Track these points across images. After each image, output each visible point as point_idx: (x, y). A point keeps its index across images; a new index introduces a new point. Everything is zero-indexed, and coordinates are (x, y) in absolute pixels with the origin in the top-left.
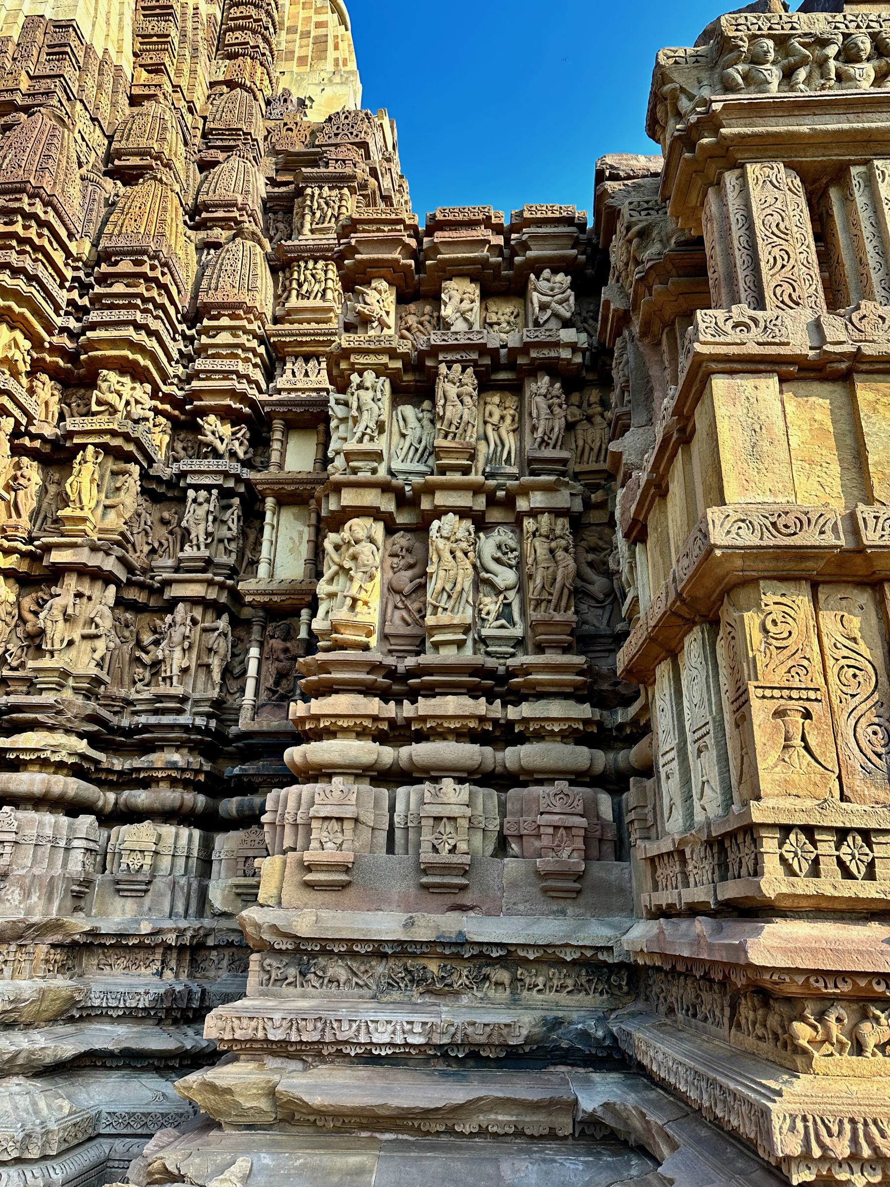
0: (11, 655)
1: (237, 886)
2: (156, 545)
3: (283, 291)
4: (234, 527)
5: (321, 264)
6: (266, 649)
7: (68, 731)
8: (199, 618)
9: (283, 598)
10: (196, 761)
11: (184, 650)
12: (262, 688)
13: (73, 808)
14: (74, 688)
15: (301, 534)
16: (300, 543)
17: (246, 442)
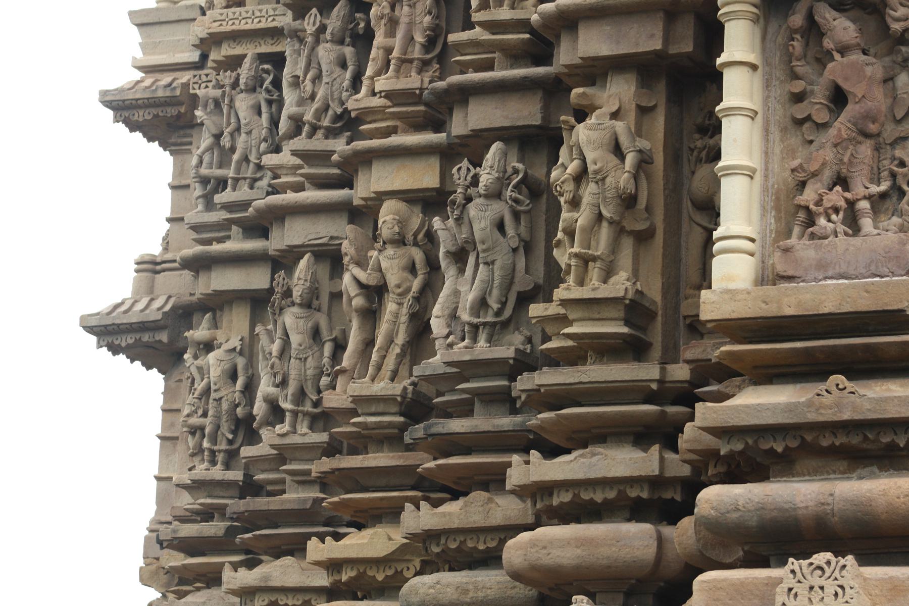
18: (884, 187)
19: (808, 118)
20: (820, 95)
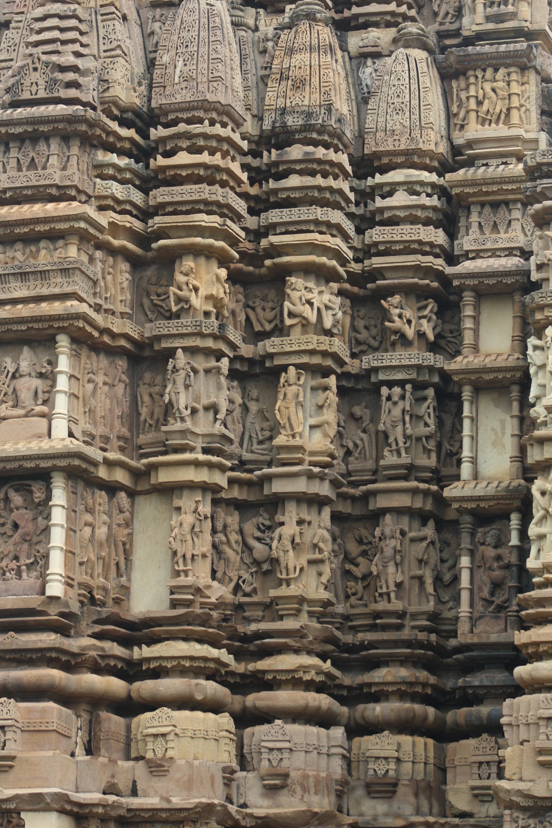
0: (244, 582)
1: (473, 788)
2: (351, 445)
3: (460, 107)
4: (431, 421)
5: (502, 71)
6: (478, 556)
7: (309, 653)
8: (406, 529)
9: (492, 503)
10: (423, 675)
11: (397, 564)
12: (476, 598)
13: (324, 720)
14: (309, 612)
15: (503, 423)
16: (503, 434)
17: (434, 317)
18: (31, 561)
19: (5, 533)
20: (9, 526)
